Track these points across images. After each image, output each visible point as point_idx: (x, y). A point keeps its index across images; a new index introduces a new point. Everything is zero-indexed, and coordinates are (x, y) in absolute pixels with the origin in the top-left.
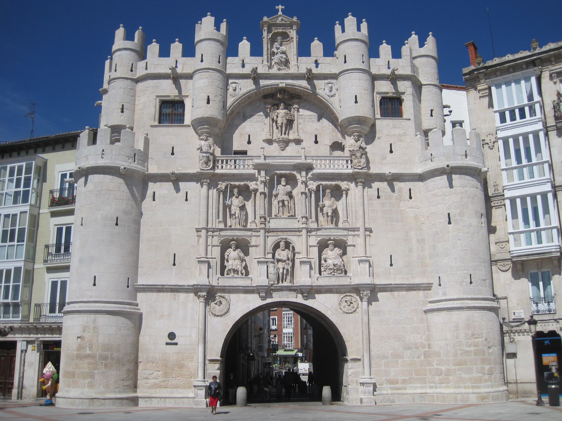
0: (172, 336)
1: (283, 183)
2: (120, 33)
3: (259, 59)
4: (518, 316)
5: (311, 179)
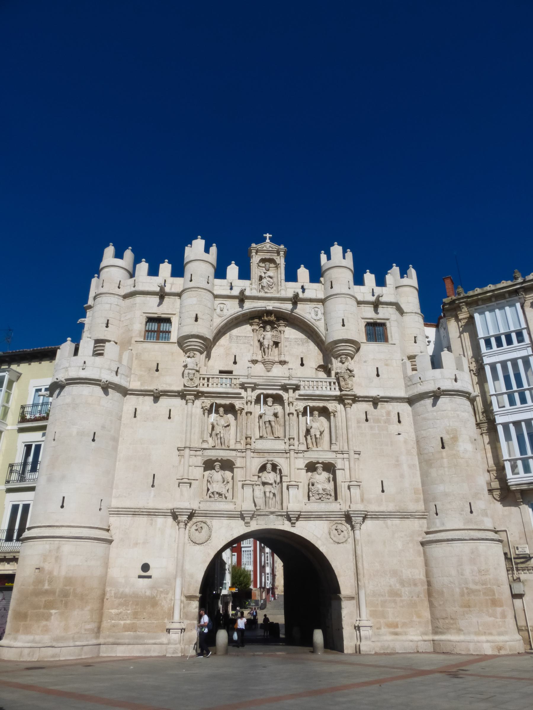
0: (146, 567)
1: (270, 403)
2: (110, 251)
4: (522, 552)
5: (297, 399)
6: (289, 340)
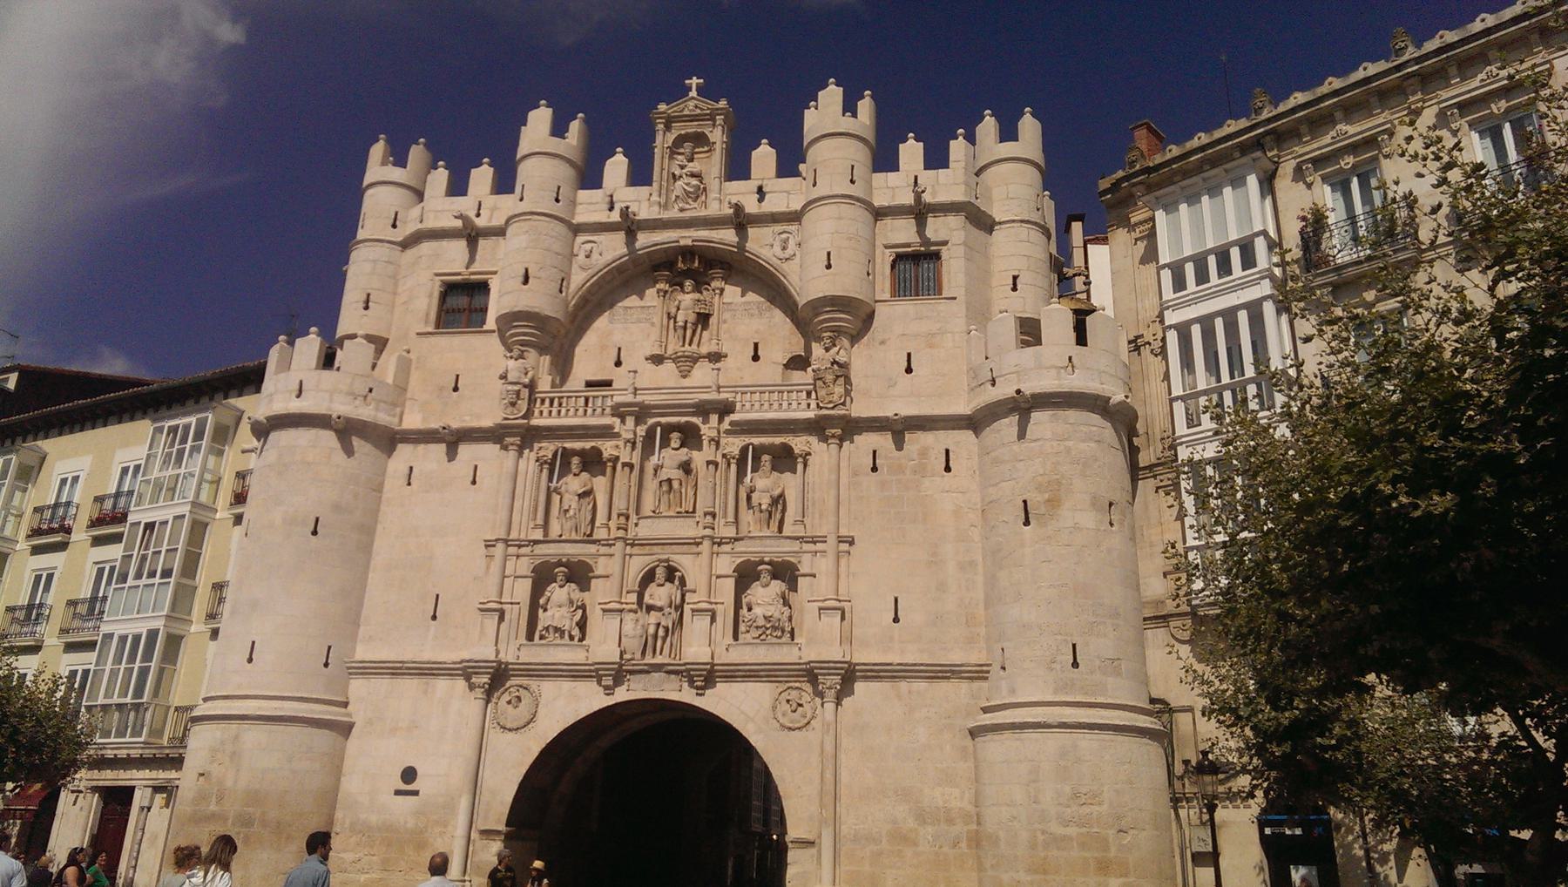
0: (409, 774)
1: (675, 443)
2: (378, 150)
3: (645, 190)
5: (728, 432)
6: (733, 307)
